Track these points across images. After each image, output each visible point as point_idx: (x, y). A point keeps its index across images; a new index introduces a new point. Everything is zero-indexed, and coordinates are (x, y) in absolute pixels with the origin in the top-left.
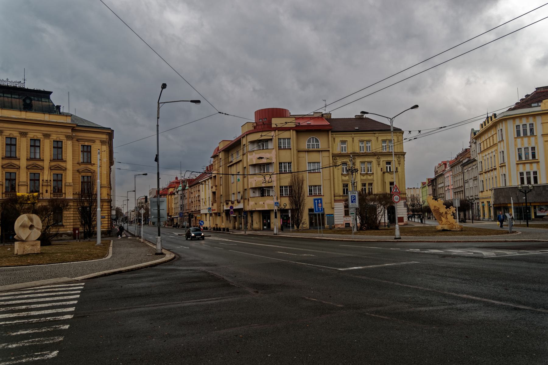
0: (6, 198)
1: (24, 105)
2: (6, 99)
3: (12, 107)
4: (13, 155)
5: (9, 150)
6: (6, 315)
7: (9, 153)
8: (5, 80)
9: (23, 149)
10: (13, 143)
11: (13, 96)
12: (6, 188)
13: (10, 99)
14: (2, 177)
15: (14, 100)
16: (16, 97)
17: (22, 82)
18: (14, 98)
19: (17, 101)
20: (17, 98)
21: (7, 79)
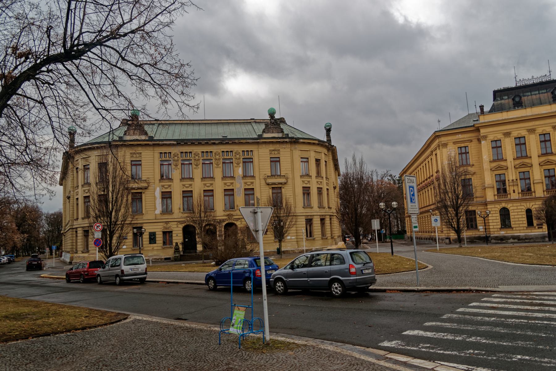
0: (548, 195)
1: (553, 98)
2: (534, 97)
3: (541, 103)
4: (549, 151)
5: (544, 146)
6: (481, 310)
7: (520, 152)
8: (530, 78)
9: (534, 146)
10: (547, 138)
11: (541, 92)
12: (547, 185)
13: (538, 96)
14: (541, 175)
15: (542, 96)
16: (544, 91)
17: (548, 74)
18: (542, 93)
19: (546, 95)
20: (545, 93)
21: (533, 77)
